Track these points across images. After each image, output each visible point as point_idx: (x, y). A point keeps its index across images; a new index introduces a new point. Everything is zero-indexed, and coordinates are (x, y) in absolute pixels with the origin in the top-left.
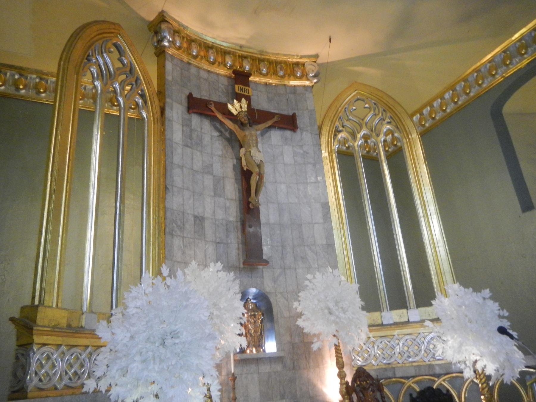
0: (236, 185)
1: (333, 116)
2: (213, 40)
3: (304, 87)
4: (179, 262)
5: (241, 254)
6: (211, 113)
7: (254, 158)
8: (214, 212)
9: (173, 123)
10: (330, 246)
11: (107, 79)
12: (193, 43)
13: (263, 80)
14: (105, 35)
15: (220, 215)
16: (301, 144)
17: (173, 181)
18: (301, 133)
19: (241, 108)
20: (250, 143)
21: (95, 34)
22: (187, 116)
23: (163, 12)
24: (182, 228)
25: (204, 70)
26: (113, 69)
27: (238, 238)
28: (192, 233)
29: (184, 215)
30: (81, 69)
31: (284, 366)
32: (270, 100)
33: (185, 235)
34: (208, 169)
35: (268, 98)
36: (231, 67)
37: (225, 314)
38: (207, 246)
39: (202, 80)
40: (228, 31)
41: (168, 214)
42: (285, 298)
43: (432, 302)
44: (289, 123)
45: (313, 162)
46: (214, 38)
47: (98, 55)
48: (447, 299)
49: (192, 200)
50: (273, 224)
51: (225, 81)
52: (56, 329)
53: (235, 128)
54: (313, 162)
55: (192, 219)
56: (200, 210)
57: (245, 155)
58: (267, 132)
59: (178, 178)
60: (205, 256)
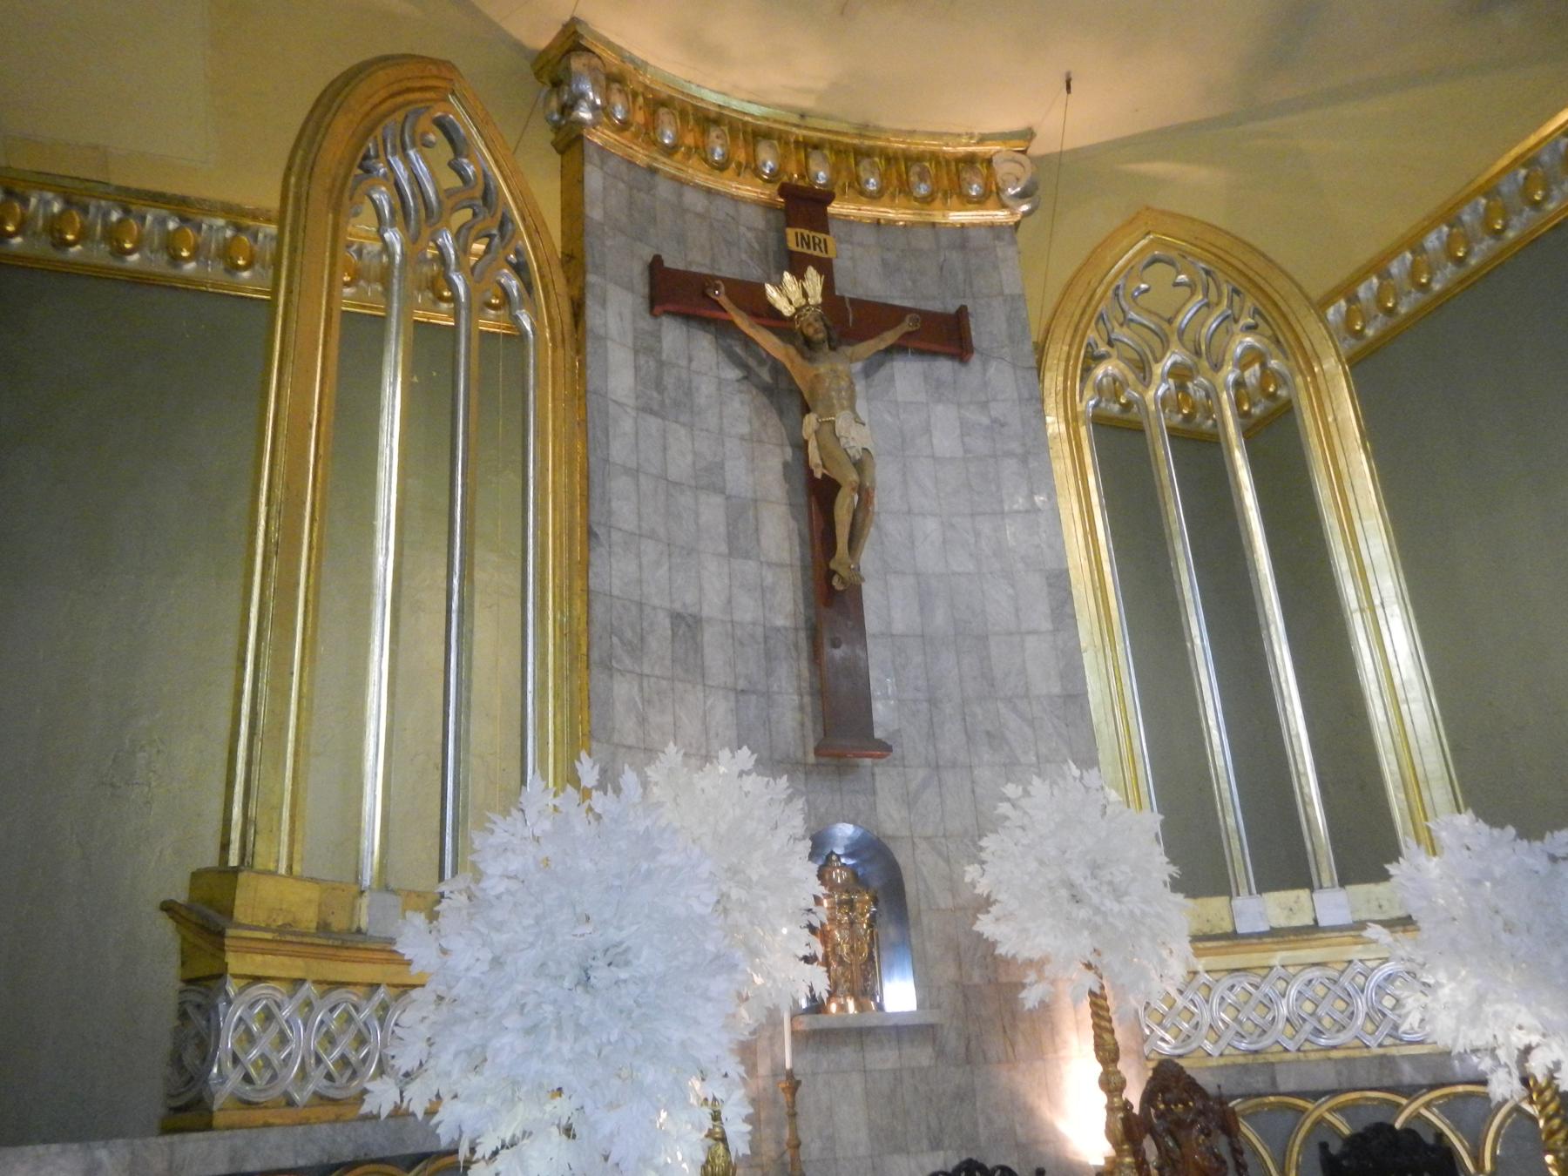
0: (793, 524)
1: (1078, 312)
2: (720, 100)
3: (992, 227)
4: (630, 748)
5: (809, 725)
7: (843, 441)
8: (729, 602)
9: (609, 343)
10: (1074, 698)
11: (418, 222)
12: (662, 111)
13: (869, 211)
14: (411, 96)
15: (748, 610)
17: (610, 513)
18: (985, 364)
19: (805, 295)
20: (830, 398)
21: (383, 94)
22: (647, 323)
23: (574, 21)
24: (637, 649)
25: (697, 187)
26: (437, 193)
27: (799, 676)
28: (668, 662)
29: (641, 610)
30: (347, 194)
31: (940, 1053)
32: (889, 270)
33: (647, 670)
35: (884, 263)
36: (774, 176)
37: (764, 898)
40: (763, 74)
41: (598, 609)
42: (940, 854)
43: (1387, 866)
44: (946, 336)
46: (724, 94)
47: (394, 154)
48: (1435, 859)
49: (663, 571)
50: (902, 636)
51: (757, 219)
52: (286, 938)
53: (787, 355)
55: (667, 622)
56: (690, 598)
57: (816, 432)
58: (881, 365)
59: (623, 504)
60: (706, 731)
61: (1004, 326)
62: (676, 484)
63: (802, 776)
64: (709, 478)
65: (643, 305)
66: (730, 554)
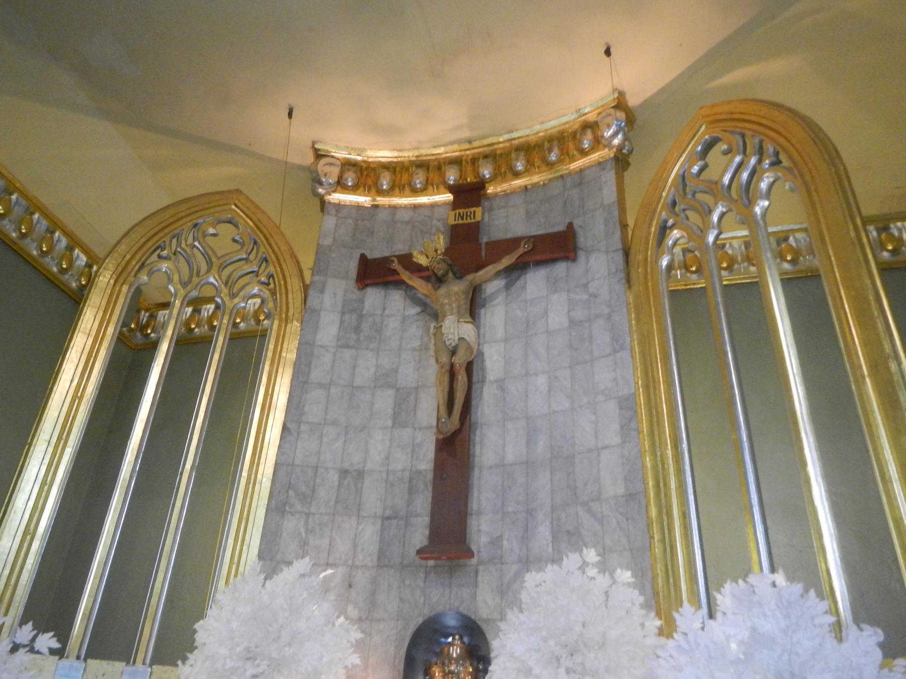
2: (417, 153)
3: (600, 164)
6: (397, 277)
8: (387, 458)
9: (322, 313)
13: (519, 182)
15: (401, 461)
16: (585, 281)
18: (588, 259)
22: (355, 294)
24: (307, 498)
28: (332, 503)
29: (316, 472)
33: (313, 510)
34: (385, 379)
35: (528, 212)
38: (360, 528)
39: (399, 225)
43: (31, 623)
45: (606, 311)
46: (418, 148)
49: (339, 444)
50: (511, 465)
54: (606, 311)
56: (357, 459)
60: (355, 546)
61: (602, 227)
62: (359, 387)
63: (422, 576)
64: (385, 379)
65: (352, 283)
66: (393, 426)
